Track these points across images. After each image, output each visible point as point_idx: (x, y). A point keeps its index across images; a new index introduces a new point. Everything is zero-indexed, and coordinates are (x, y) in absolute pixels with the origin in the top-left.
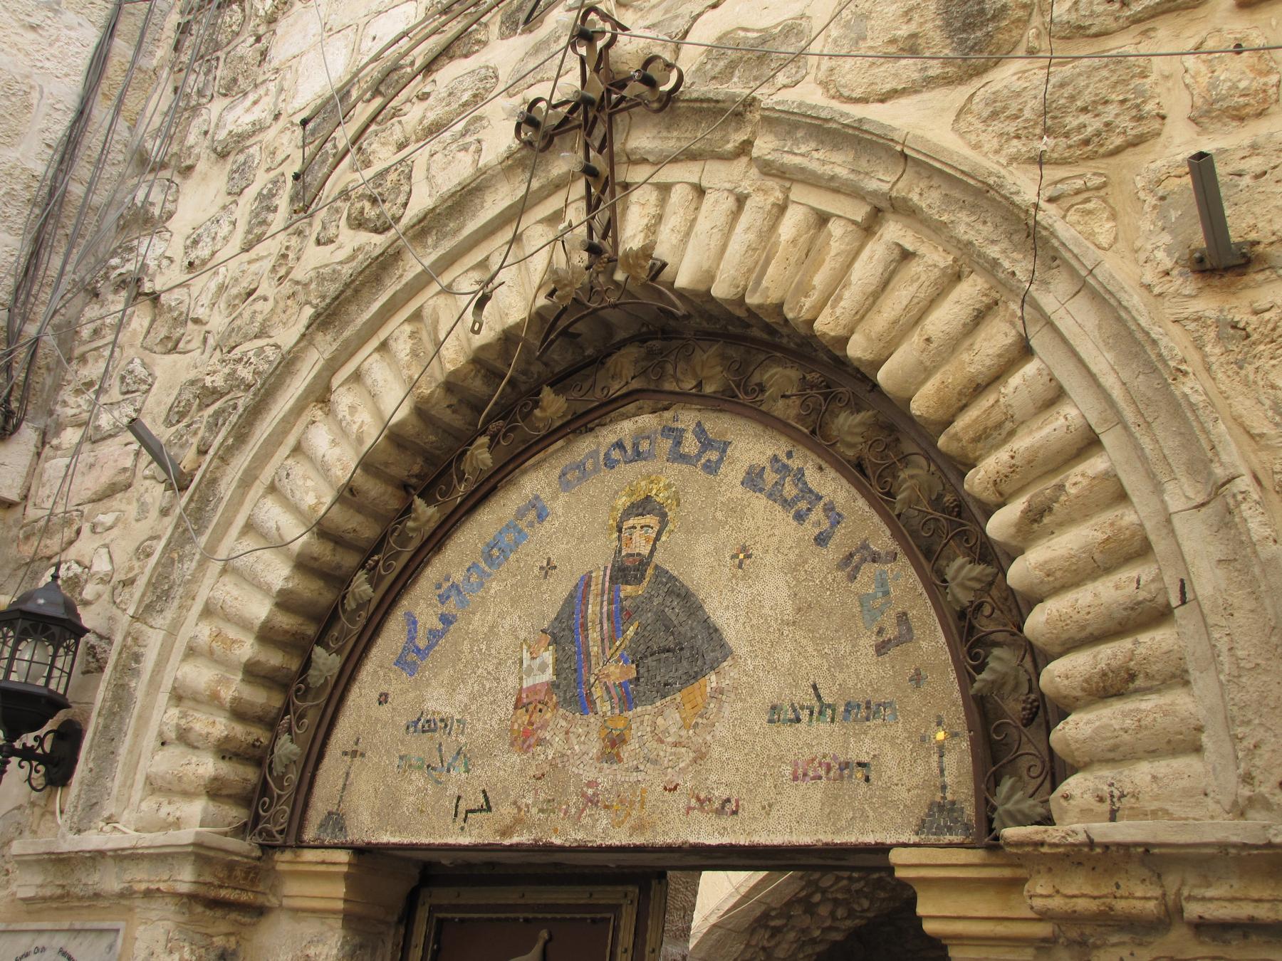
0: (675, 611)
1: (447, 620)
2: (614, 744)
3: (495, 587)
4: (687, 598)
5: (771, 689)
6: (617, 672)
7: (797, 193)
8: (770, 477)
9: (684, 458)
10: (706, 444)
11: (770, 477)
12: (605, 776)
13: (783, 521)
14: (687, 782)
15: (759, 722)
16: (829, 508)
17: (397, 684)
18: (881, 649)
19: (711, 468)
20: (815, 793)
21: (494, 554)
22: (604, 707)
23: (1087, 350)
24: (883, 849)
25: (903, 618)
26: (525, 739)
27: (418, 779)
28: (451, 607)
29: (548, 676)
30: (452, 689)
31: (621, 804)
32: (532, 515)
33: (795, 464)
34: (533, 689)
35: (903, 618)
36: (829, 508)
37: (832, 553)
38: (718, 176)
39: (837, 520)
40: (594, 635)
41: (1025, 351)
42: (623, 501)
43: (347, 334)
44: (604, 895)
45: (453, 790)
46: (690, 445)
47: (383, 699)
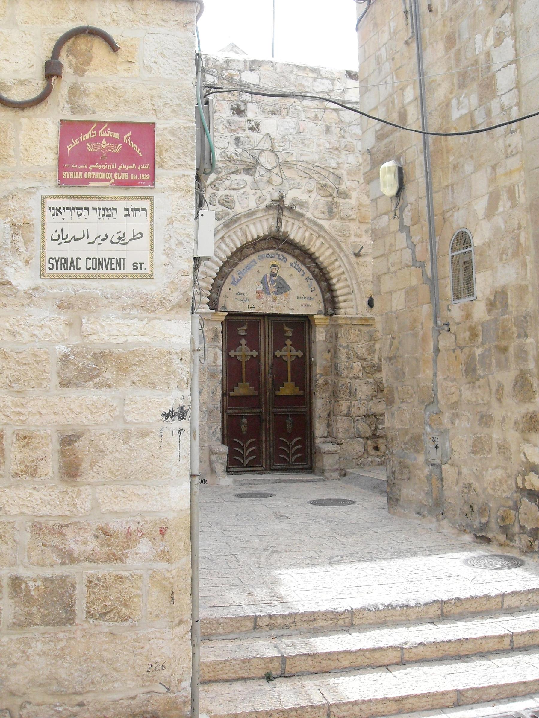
0: (282, 281)
1: (241, 278)
2: (275, 300)
3: (249, 273)
4: (283, 280)
5: (297, 294)
6: (274, 290)
7: (308, 229)
8: (294, 265)
9: (280, 259)
10: (284, 258)
11: (294, 265)
12: (274, 304)
13: (297, 272)
14: (287, 306)
15: (296, 299)
16: (303, 271)
17: (232, 287)
18: (312, 291)
19: (285, 262)
20: (304, 308)
21: (248, 268)
22: (272, 294)
23: (345, 263)
24: (313, 315)
25: (314, 288)
26: (259, 298)
27: (240, 302)
28: (241, 275)
29: (262, 289)
30: (244, 288)
31: (277, 308)
32: (253, 263)
33: (297, 263)
34: (259, 291)
35: (314, 288)
36: (303, 271)
37: (304, 278)
38: (297, 223)
39: (304, 273)
40: (269, 284)
41: (336, 260)
42: (271, 264)
43: (230, 229)
44: (258, 318)
45: (247, 304)
46: (281, 257)
47: (230, 289)
